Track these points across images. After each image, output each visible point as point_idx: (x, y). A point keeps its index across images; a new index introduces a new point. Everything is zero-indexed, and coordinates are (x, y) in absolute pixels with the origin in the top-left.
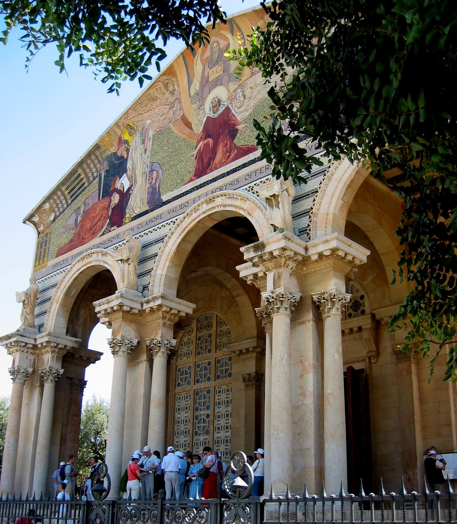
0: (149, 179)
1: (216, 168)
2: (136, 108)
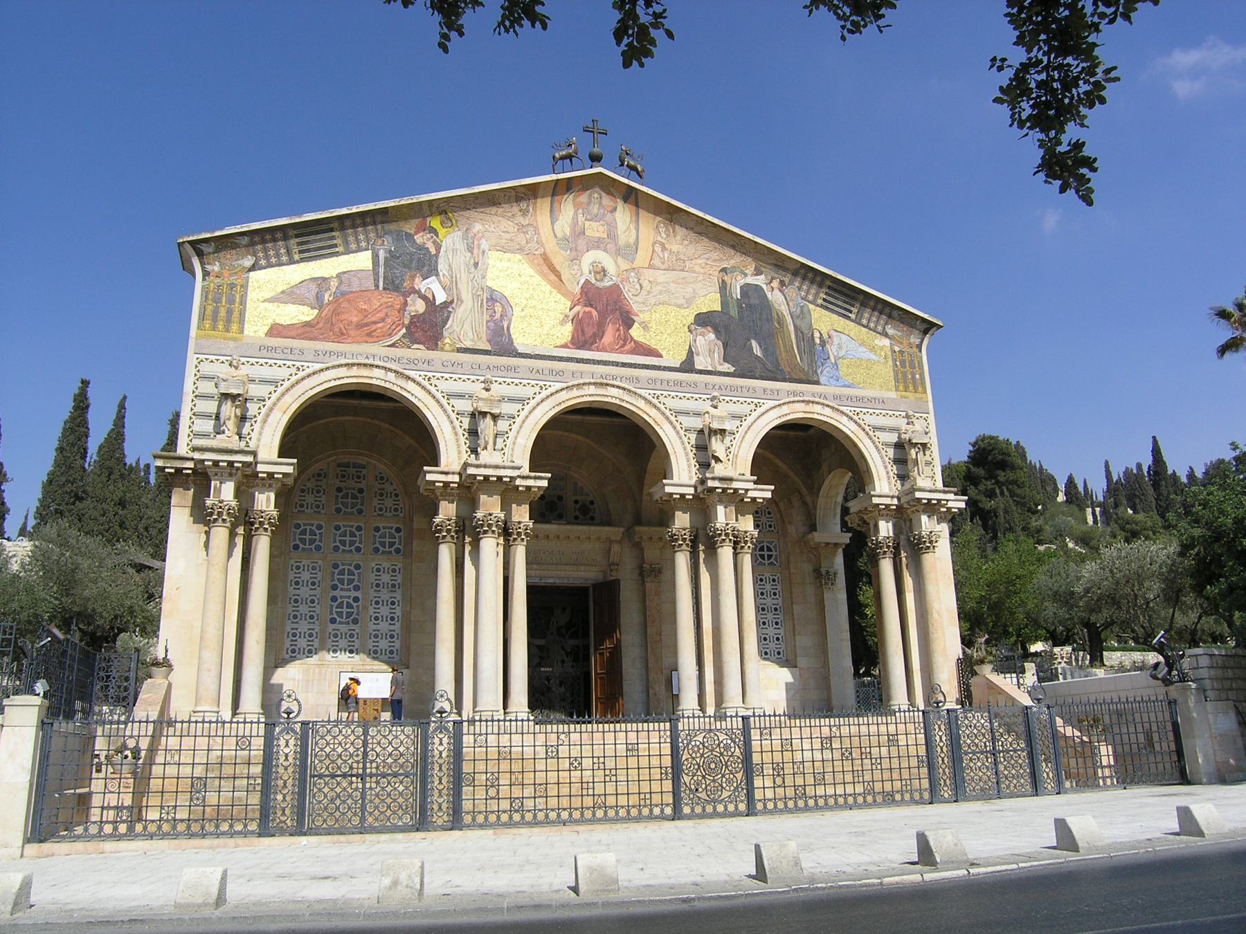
1: (604, 350)
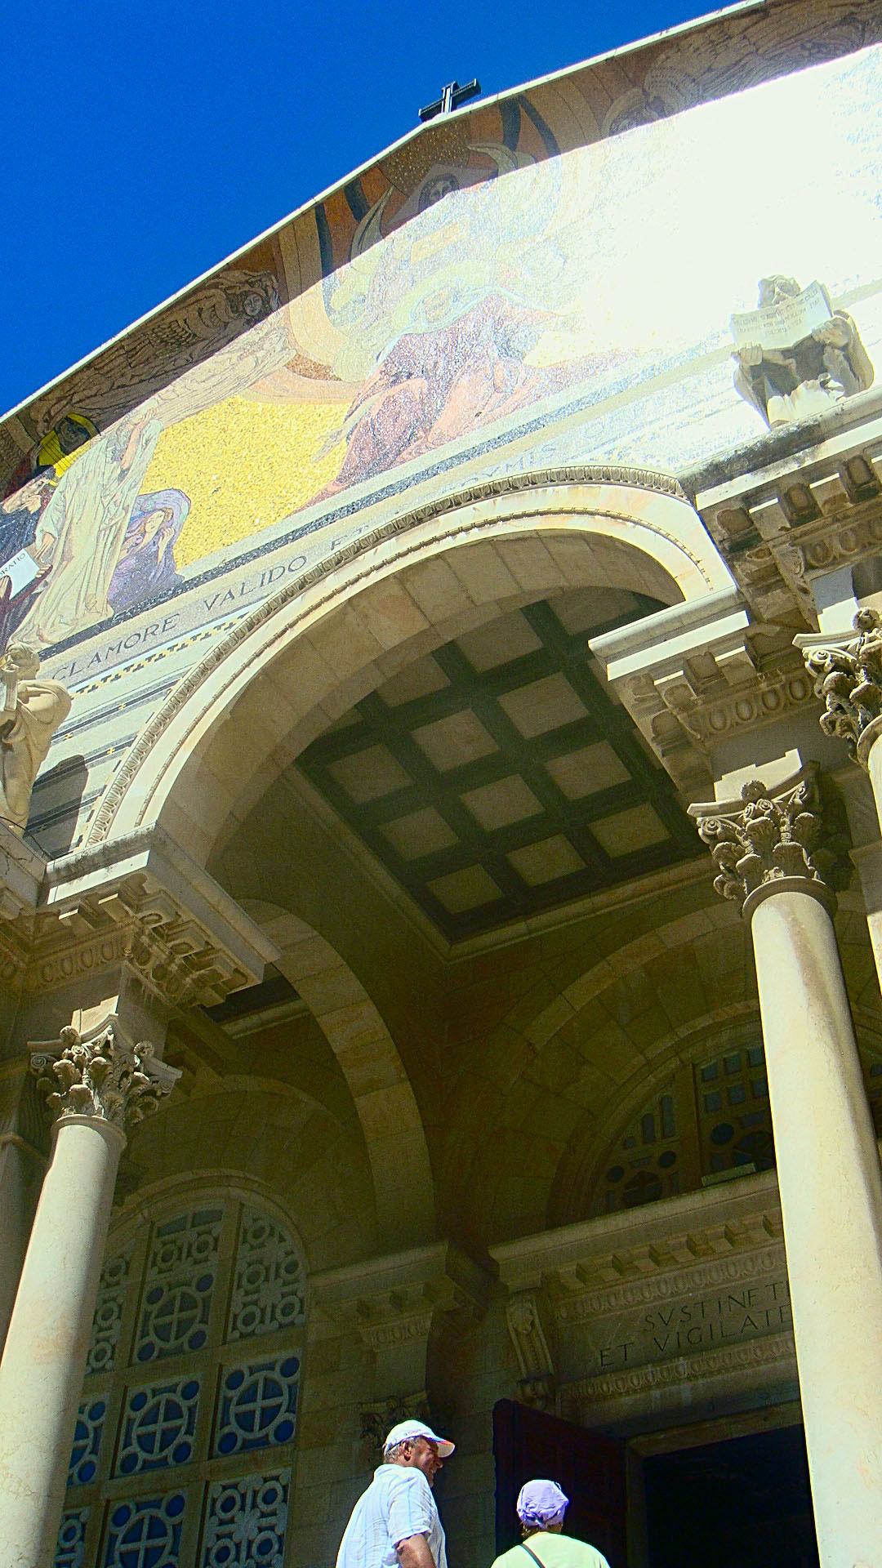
0: (126, 539)
1: (440, 441)
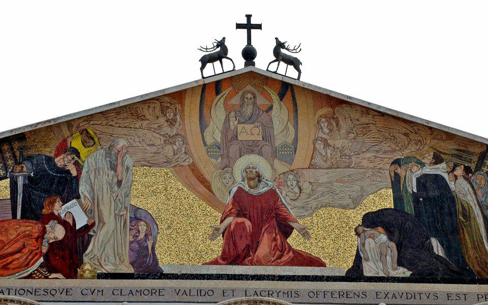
1: (259, 263)
2: (109, 115)
